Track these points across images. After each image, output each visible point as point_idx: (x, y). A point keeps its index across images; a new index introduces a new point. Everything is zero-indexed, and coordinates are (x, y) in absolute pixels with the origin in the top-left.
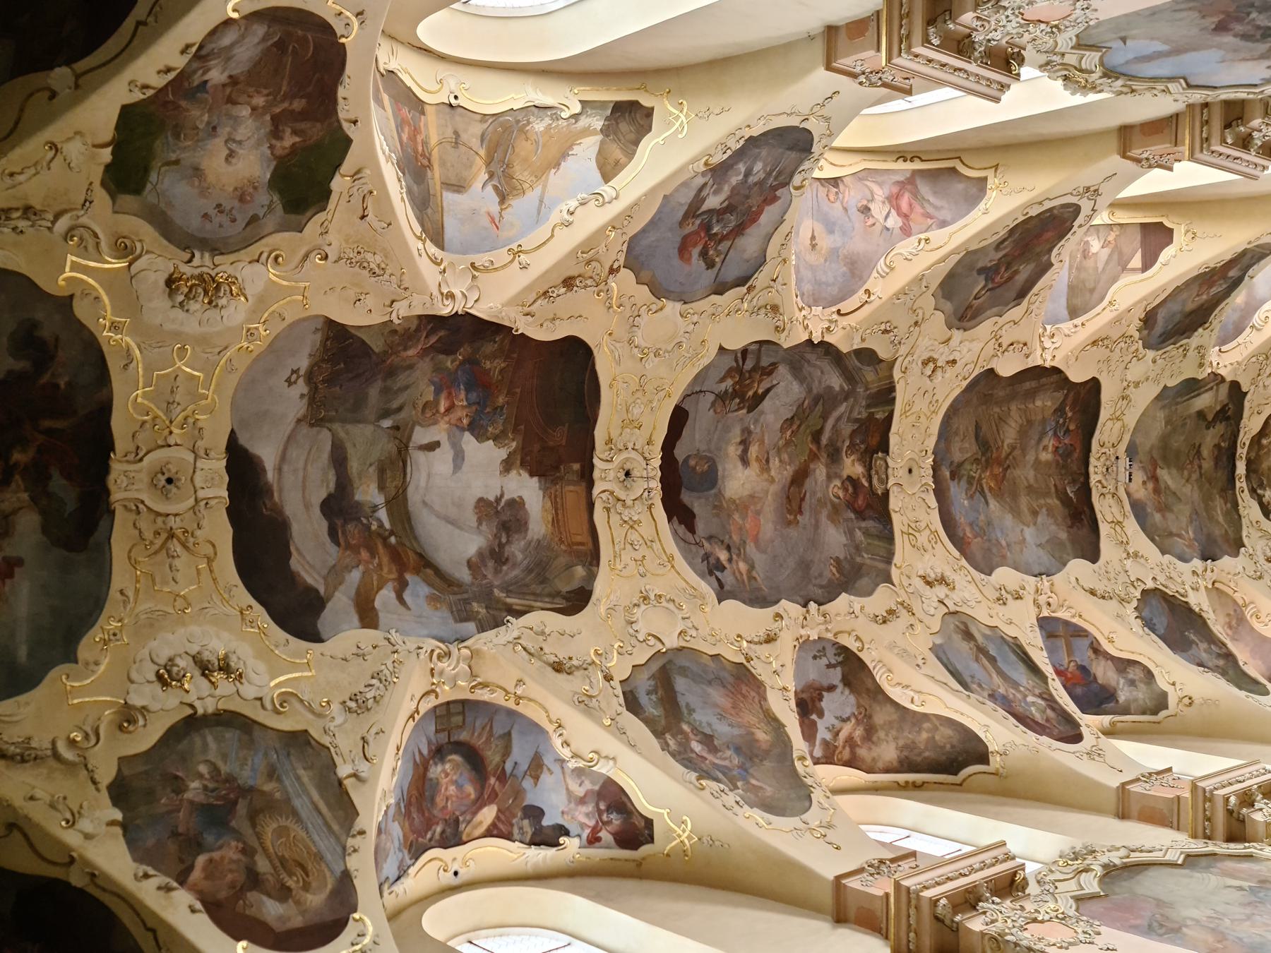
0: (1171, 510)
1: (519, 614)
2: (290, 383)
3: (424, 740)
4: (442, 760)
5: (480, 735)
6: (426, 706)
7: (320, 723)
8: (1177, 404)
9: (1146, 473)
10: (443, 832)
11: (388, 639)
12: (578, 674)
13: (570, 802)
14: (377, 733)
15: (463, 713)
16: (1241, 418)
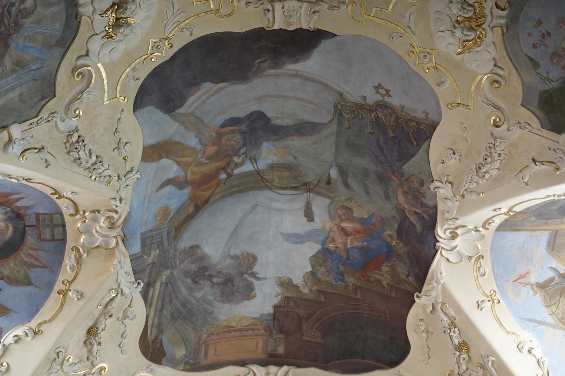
1: (145, 295)
2: (377, 88)
3: (31, 203)
4: (8, 219)
5: (31, 255)
6: (65, 207)
7: (61, 110)
11: (131, 171)
12: (84, 352)
14: (46, 161)
15: (53, 240)
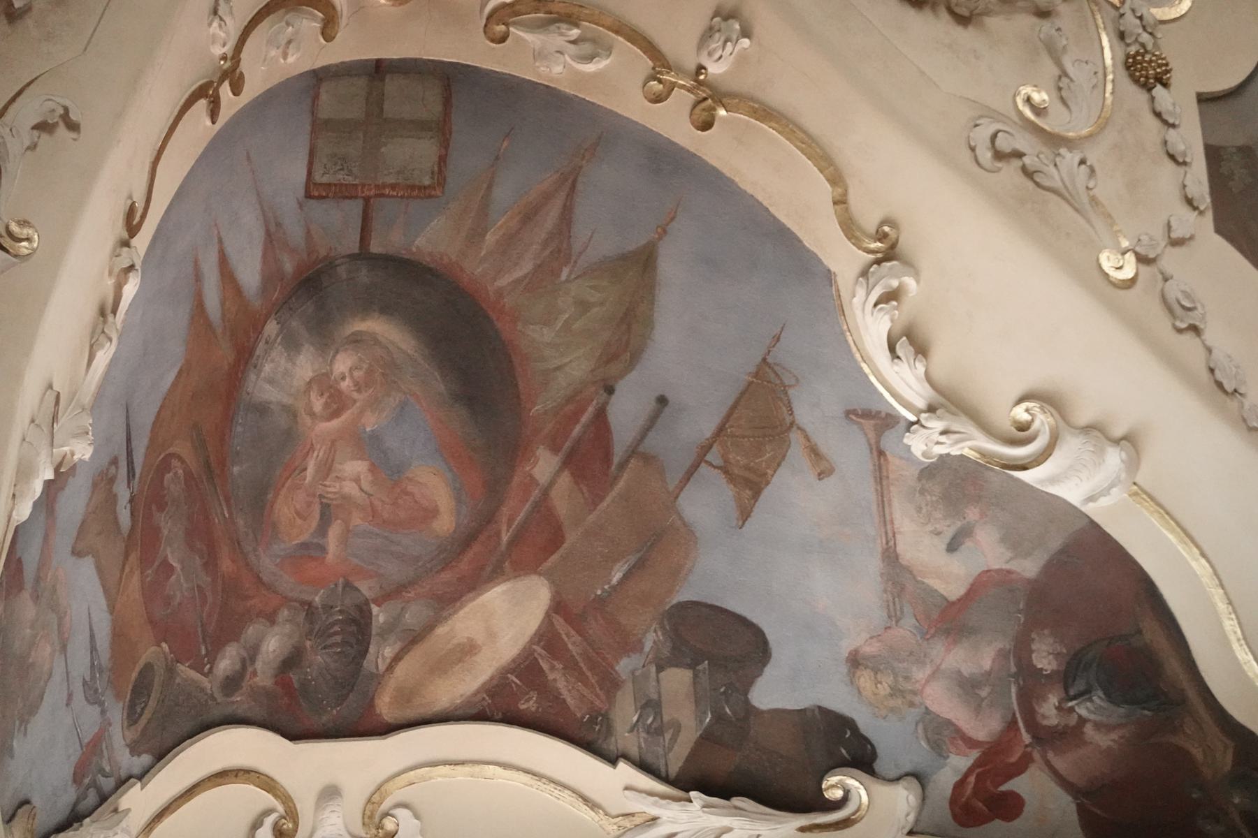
3: (251, 220)
5: (510, 241)
10: (291, 661)
13: (894, 617)
15: (441, 130)
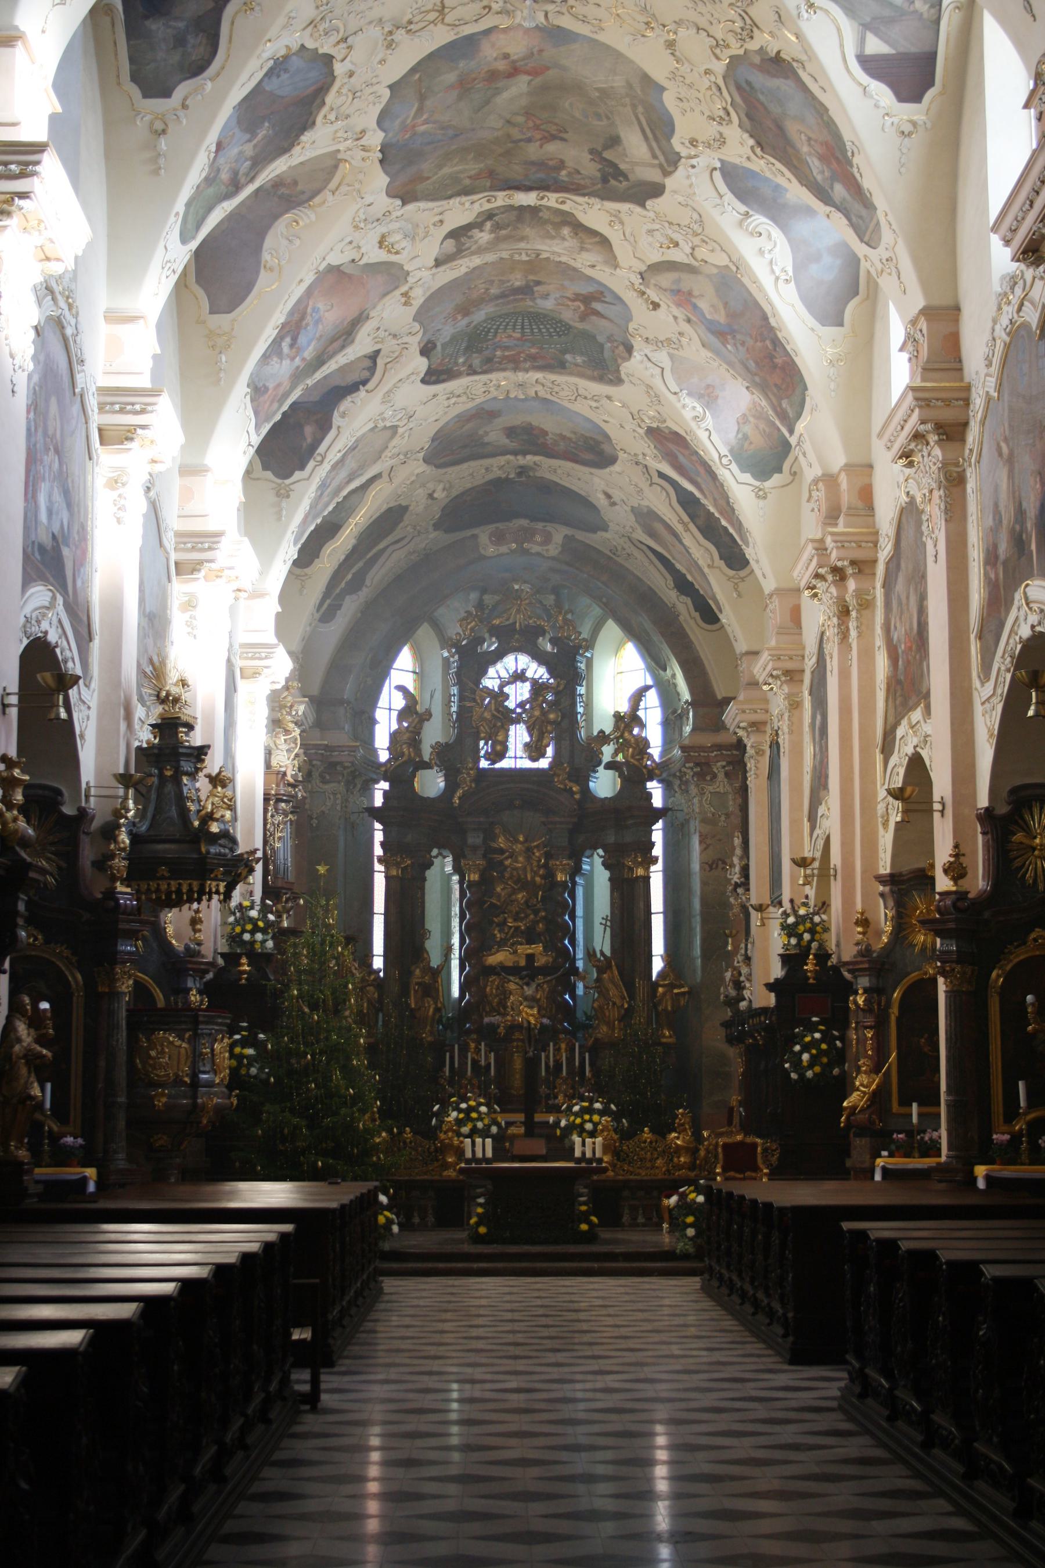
0: (460, 98)
8: (634, 107)
9: (523, 59)
16: (602, 199)
